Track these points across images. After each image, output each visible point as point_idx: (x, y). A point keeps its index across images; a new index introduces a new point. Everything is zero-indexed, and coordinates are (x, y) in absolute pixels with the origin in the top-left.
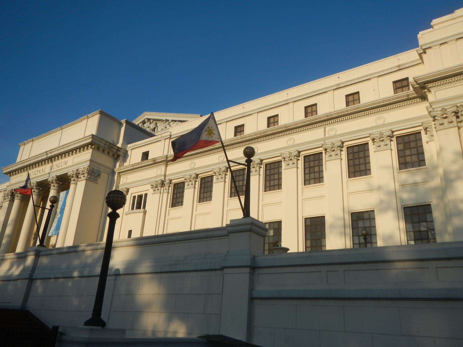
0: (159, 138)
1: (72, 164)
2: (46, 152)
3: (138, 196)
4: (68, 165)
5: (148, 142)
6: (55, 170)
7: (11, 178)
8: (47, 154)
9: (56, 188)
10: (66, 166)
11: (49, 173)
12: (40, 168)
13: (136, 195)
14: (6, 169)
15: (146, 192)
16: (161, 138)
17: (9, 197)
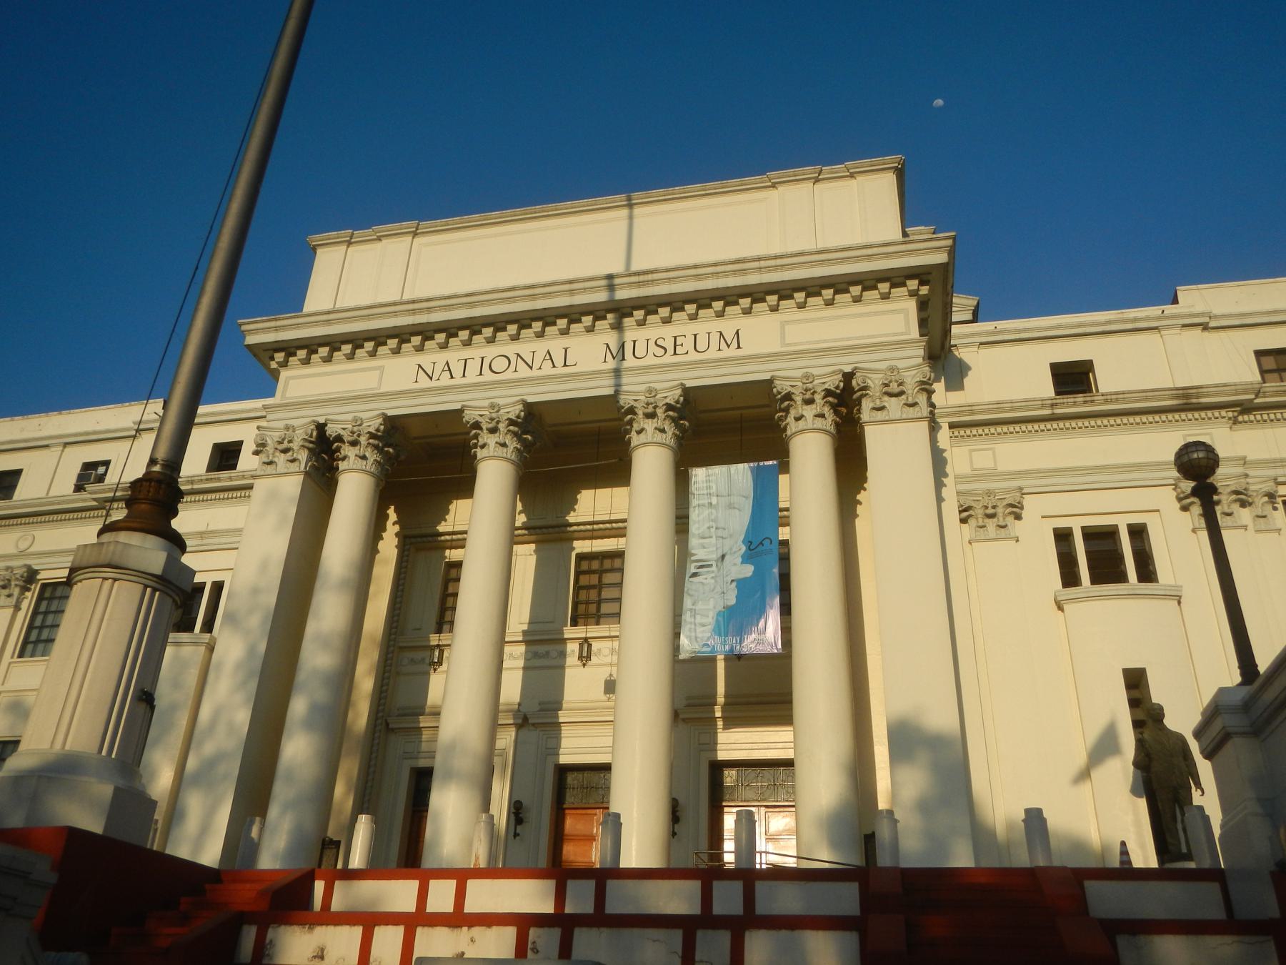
0: (1148, 319)
1: (776, 348)
2: (610, 277)
3: (1083, 528)
4: (747, 350)
5: (1080, 325)
6: (650, 360)
7: (284, 374)
8: (611, 288)
9: (669, 438)
11: (617, 372)
12: (530, 346)
13: (1076, 526)
14: (277, 329)
15: (1136, 519)
16: (1158, 318)
17: (303, 456)
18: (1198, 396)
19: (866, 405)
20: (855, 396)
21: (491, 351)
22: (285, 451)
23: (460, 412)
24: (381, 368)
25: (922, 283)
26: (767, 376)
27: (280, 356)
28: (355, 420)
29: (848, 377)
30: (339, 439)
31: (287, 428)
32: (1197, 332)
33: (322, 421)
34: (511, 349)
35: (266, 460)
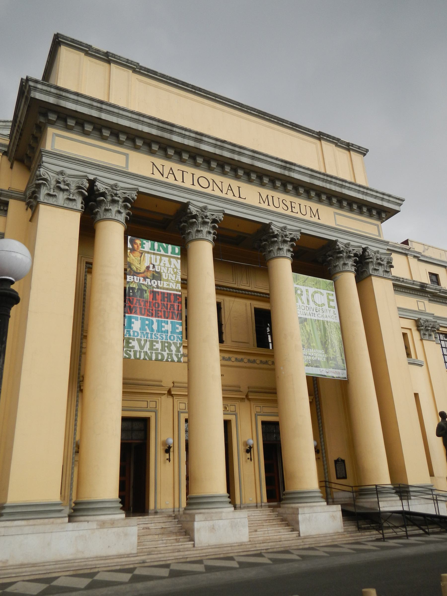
1: (333, 225)
6: (280, 210)
10: (315, 220)
17: (79, 200)
18: (426, 287)
19: (371, 267)
20: (368, 260)
21: (198, 173)
22: (63, 190)
23: (185, 206)
24: (127, 155)
25: (386, 215)
26: (334, 239)
27: (52, 117)
28: (116, 185)
29: (365, 250)
30: (103, 194)
31: (62, 173)
32: (416, 260)
33: (91, 177)
34: (210, 176)
35: (47, 192)
